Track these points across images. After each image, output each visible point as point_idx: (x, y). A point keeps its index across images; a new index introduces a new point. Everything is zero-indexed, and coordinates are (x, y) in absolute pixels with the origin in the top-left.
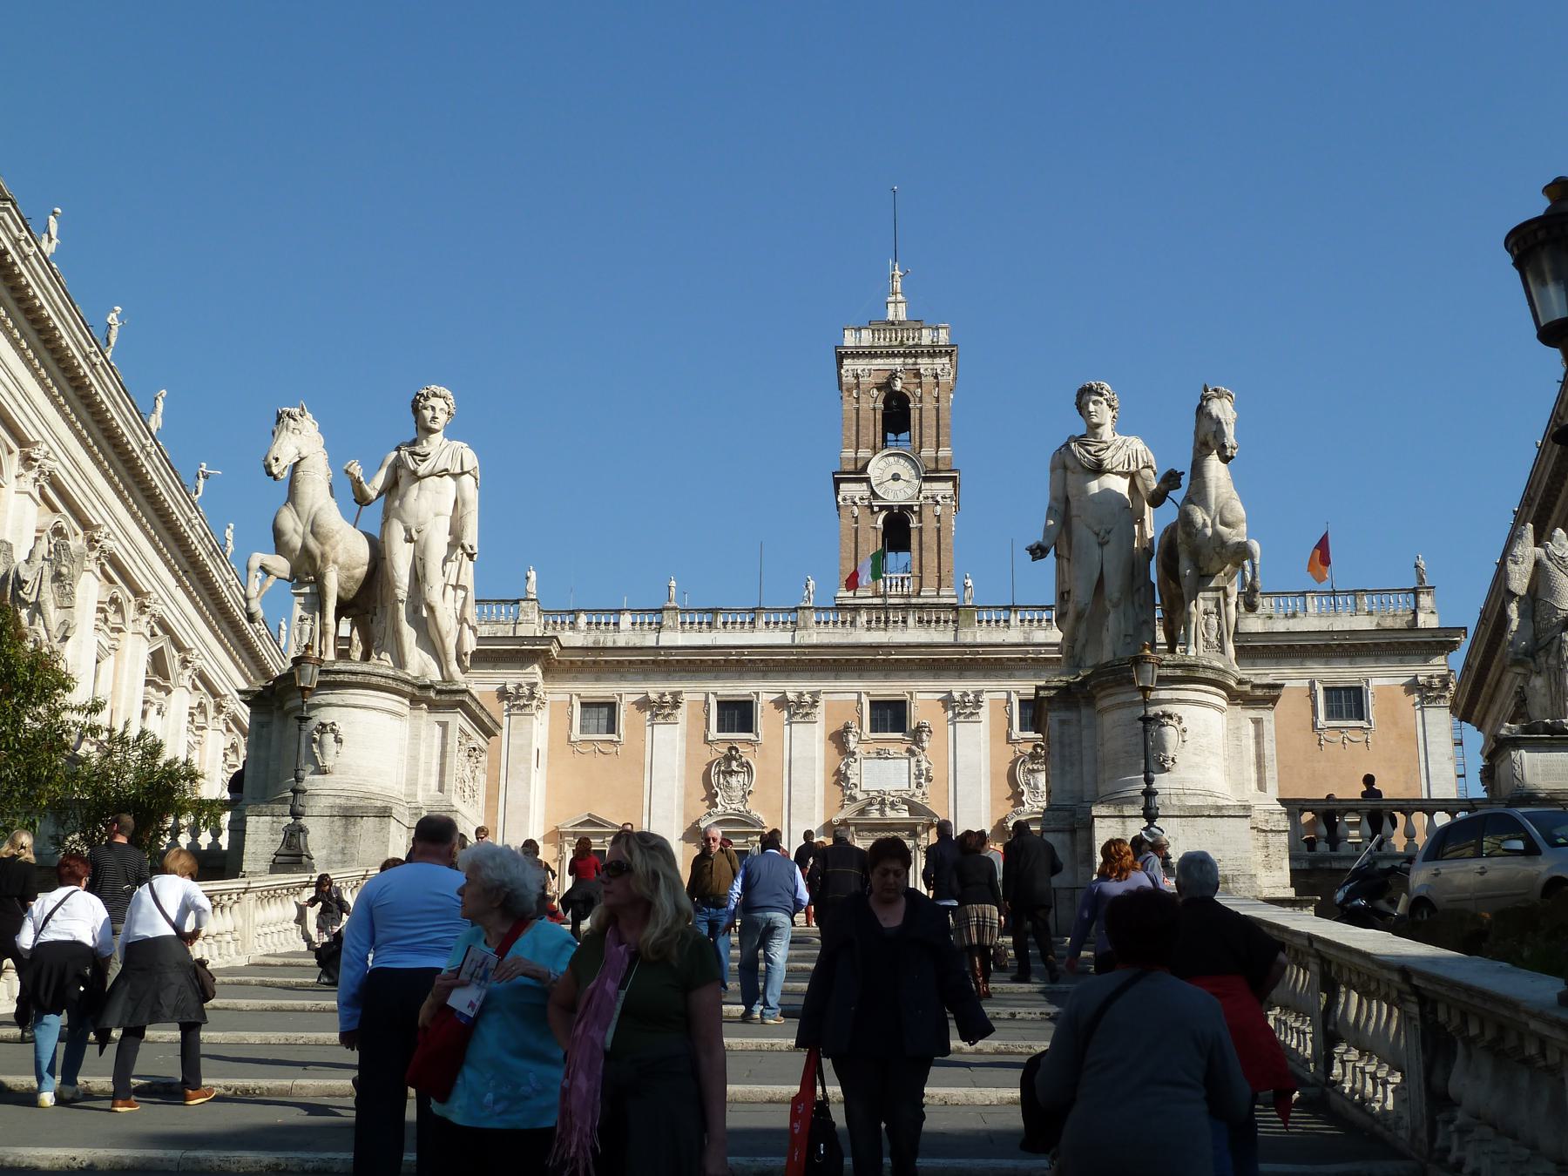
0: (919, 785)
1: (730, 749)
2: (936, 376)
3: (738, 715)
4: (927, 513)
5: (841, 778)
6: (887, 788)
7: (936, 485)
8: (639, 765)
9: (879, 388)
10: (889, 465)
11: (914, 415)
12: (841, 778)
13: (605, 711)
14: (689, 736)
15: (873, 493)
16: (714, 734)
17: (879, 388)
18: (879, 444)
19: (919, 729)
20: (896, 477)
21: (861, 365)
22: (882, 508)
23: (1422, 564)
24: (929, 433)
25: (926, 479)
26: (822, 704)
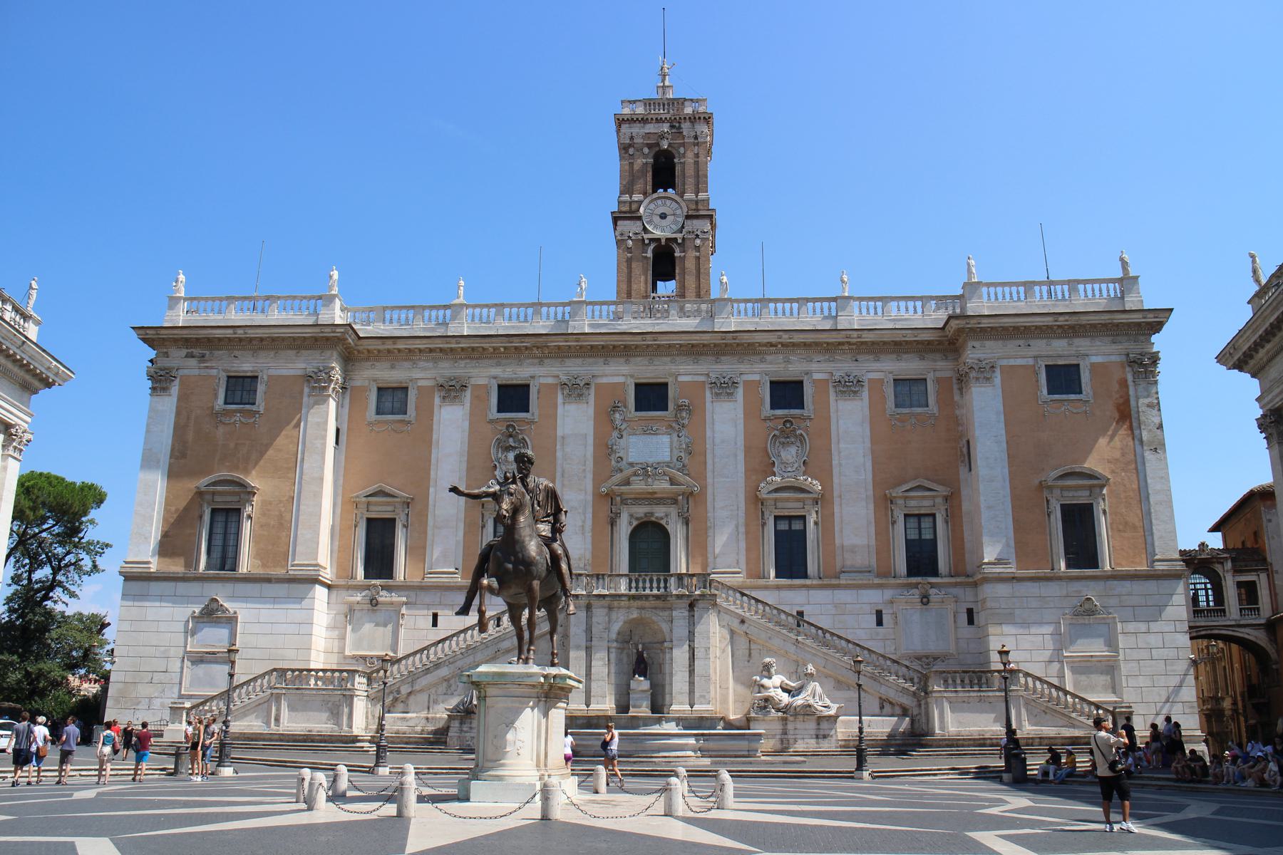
0: (679, 459)
1: (508, 427)
2: (696, 137)
3: (514, 397)
4: (688, 243)
5: (610, 450)
6: (651, 460)
7: (695, 222)
8: (425, 438)
9: (650, 146)
10: (657, 206)
11: (678, 168)
12: (605, 451)
13: (400, 394)
14: (471, 414)
15: (645, 229)
16: (493, 413)
17: (650, 146)
18: (649, 188)
19: (679, 408)
20: (663, 216)
21: (637, 130)
22: (651, 240)
23: (1126, 256)
24: (690, 181)
25: (688, 217)
26: (593, 387)
